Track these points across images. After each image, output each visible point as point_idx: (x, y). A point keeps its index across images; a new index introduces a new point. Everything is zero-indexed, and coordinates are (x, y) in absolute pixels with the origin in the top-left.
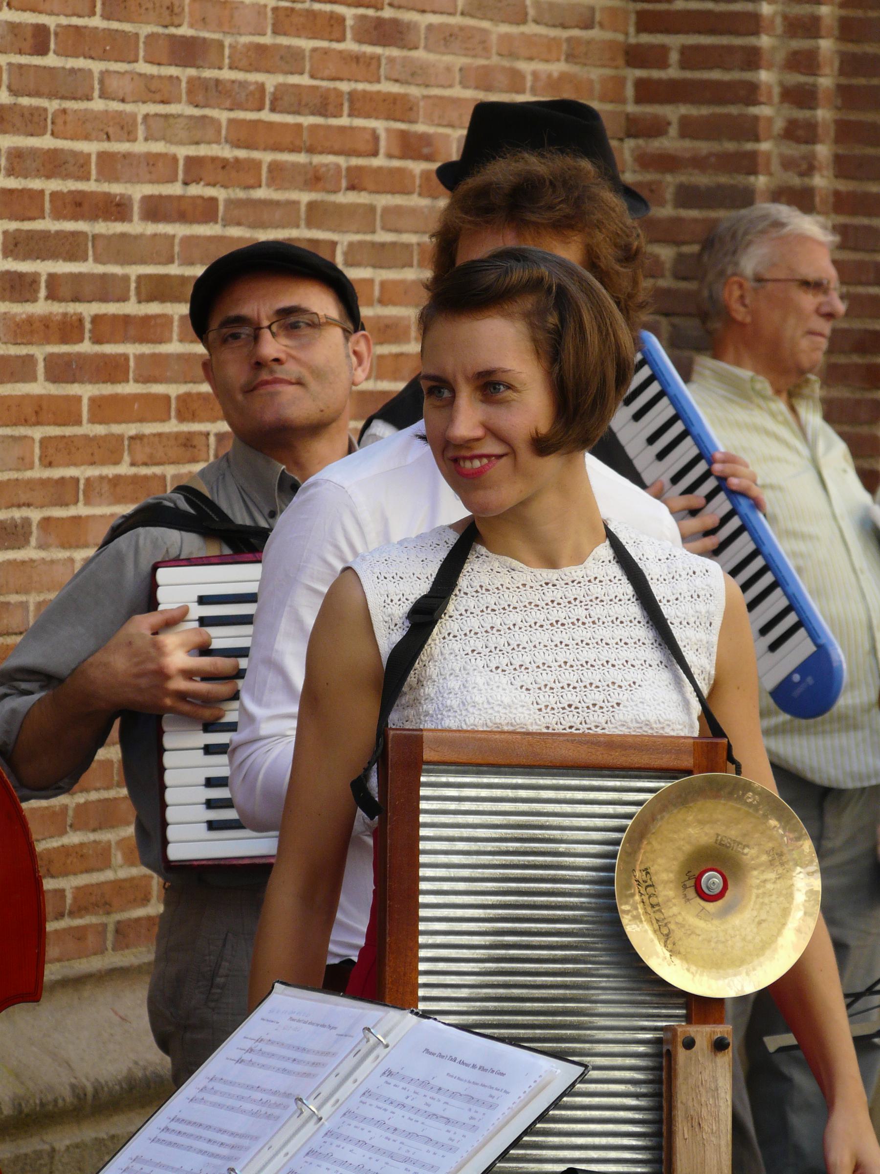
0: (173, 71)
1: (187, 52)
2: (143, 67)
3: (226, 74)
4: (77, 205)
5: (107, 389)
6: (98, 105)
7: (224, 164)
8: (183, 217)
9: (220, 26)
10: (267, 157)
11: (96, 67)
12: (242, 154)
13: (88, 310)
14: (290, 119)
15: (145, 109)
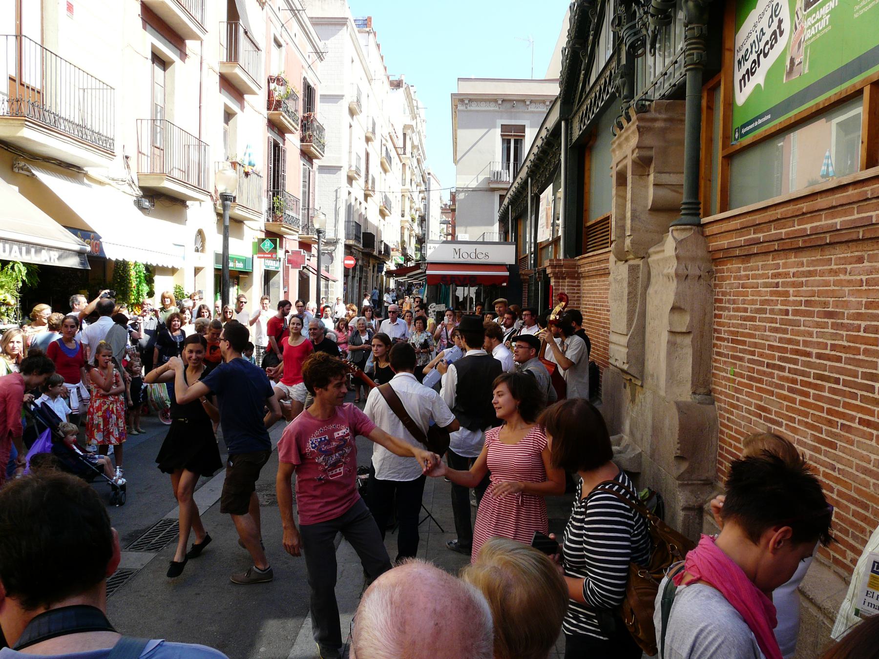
0: (826, 320)
1: (830, 315)
2: (816, 319)
3: (846, 321)
4: (797, 352)
5: (804, 399)
6: (802, 328)
7: (844, 347)
8: (829, 360)
9: (843, 307)
10: (863, 347)
11: (802, 319)
12: (852, 344)
13: (799, 378)
14: (873, 336)
15: (816, 330)
